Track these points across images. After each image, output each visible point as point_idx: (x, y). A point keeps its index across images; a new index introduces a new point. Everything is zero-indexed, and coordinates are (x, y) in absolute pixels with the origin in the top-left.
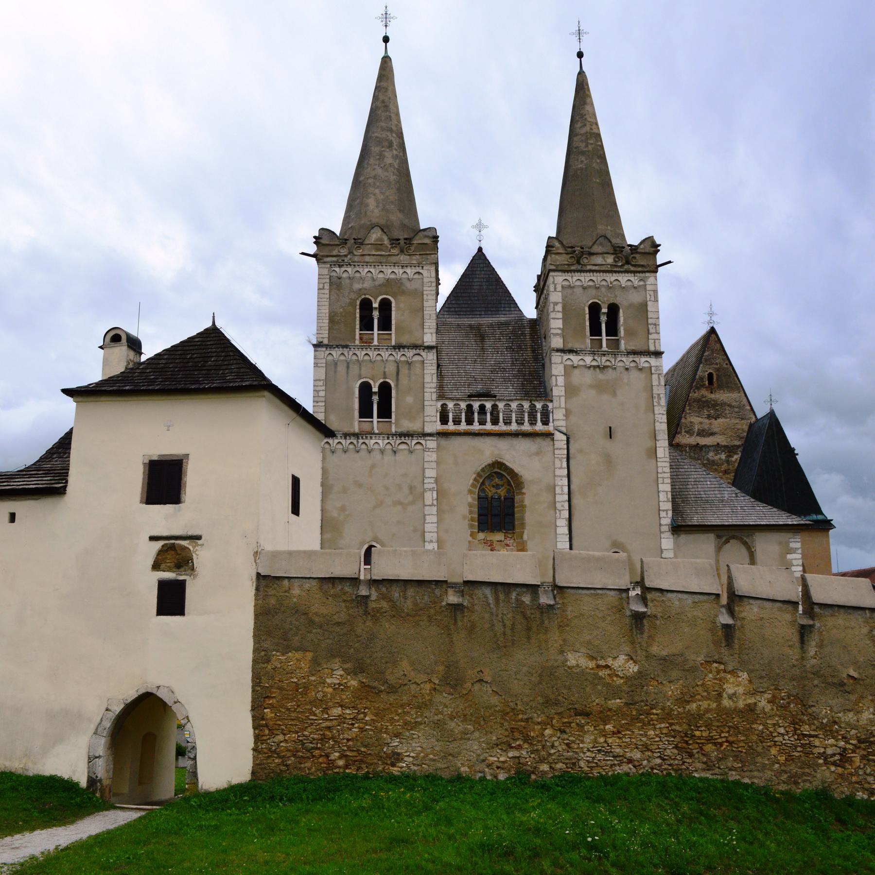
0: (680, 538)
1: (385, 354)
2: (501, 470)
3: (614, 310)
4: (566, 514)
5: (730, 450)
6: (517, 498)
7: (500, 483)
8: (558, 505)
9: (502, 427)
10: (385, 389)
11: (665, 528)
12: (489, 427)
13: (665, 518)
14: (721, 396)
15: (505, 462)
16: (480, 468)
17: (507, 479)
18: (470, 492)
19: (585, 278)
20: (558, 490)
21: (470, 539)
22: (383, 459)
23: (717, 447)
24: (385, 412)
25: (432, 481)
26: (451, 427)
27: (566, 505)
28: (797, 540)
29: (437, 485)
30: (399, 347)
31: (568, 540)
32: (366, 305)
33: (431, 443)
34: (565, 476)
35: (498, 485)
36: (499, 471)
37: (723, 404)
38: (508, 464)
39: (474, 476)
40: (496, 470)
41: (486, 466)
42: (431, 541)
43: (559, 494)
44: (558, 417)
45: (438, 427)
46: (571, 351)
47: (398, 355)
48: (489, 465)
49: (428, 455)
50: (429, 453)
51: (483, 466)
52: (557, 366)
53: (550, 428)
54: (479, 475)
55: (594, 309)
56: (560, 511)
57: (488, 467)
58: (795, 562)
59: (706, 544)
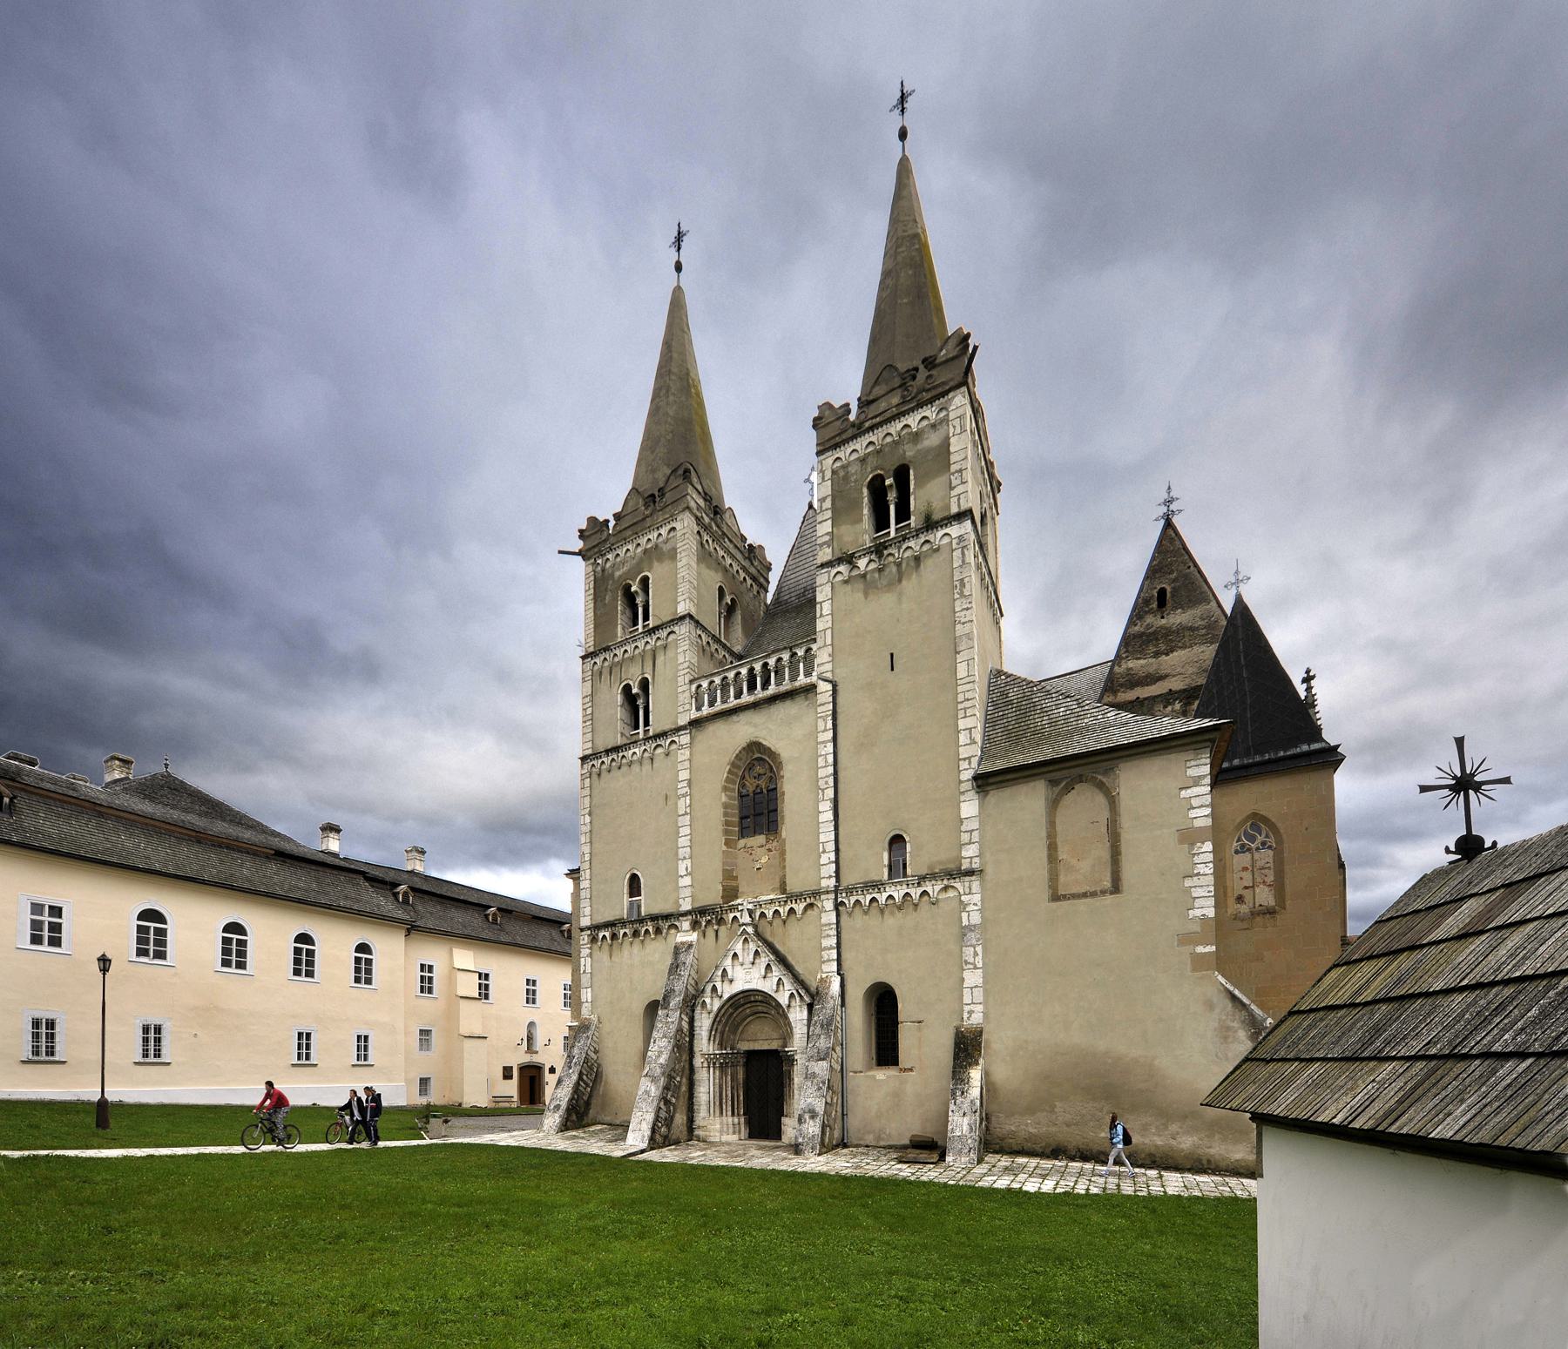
0: (989, 797)
2: (761, 754)
4: (830, 793)
7: (762, 771)
8: (821, 783)
11: (964, 787)
13: (967, 769)
15: (761, 740)
16: (734, 755)
17: (769, 764)
18: (725, 789)
20: (821, 762)
21: (724, 848)
22: (641, 770)
25: (685, 784)
27: (831, 780)
28: (1203, 761)
29: (690, 789)
31: (833, 829)
34: (829, 741)
35: (759, 775)
36: (760, 755)
38: (764, 743)
39: (728, 767)
40: (757, 755)
41: (740, 752)
42: (685, 858)
43: (822, 767)
48: (744, 748)
49: (681, 754)
50: (682, 751)
51: (737, 752)
54: (733, 764)
56: (823, 790)
57: (743, 752)
58: (1195, 802)
59: (1031, 799)
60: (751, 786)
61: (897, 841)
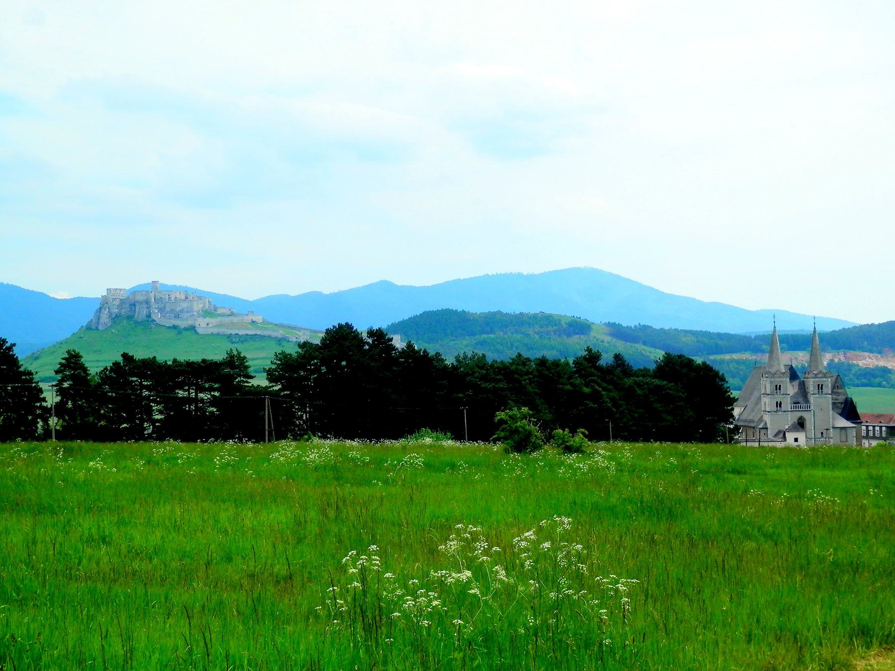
1: (781, 396)
3: (822, 385)
5: (841, 403)
6: (805, 422)
9: (802, 409)
10: (781, 402)
12: (800, 409)
14: (840, 391)
19: (817, 380)
23: (839, 403)
24: (780, 406)
26: (793, 409)
30: (783, 394)
32: (776, 386)
33: (789, 413)
37: (841, 393)
44: (812, 407)
45: (790, 410)
46: (814, 394)
47: (783, 396)
52: (812, 399)
53: (811, 409)
55: (819, 385)
60: (800, 421)
61: (822, 433)
